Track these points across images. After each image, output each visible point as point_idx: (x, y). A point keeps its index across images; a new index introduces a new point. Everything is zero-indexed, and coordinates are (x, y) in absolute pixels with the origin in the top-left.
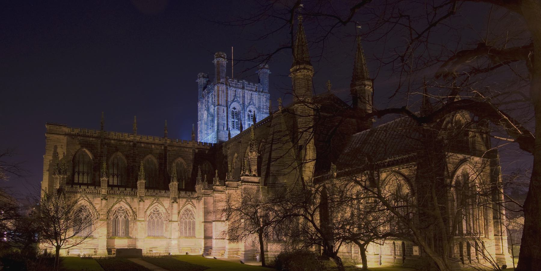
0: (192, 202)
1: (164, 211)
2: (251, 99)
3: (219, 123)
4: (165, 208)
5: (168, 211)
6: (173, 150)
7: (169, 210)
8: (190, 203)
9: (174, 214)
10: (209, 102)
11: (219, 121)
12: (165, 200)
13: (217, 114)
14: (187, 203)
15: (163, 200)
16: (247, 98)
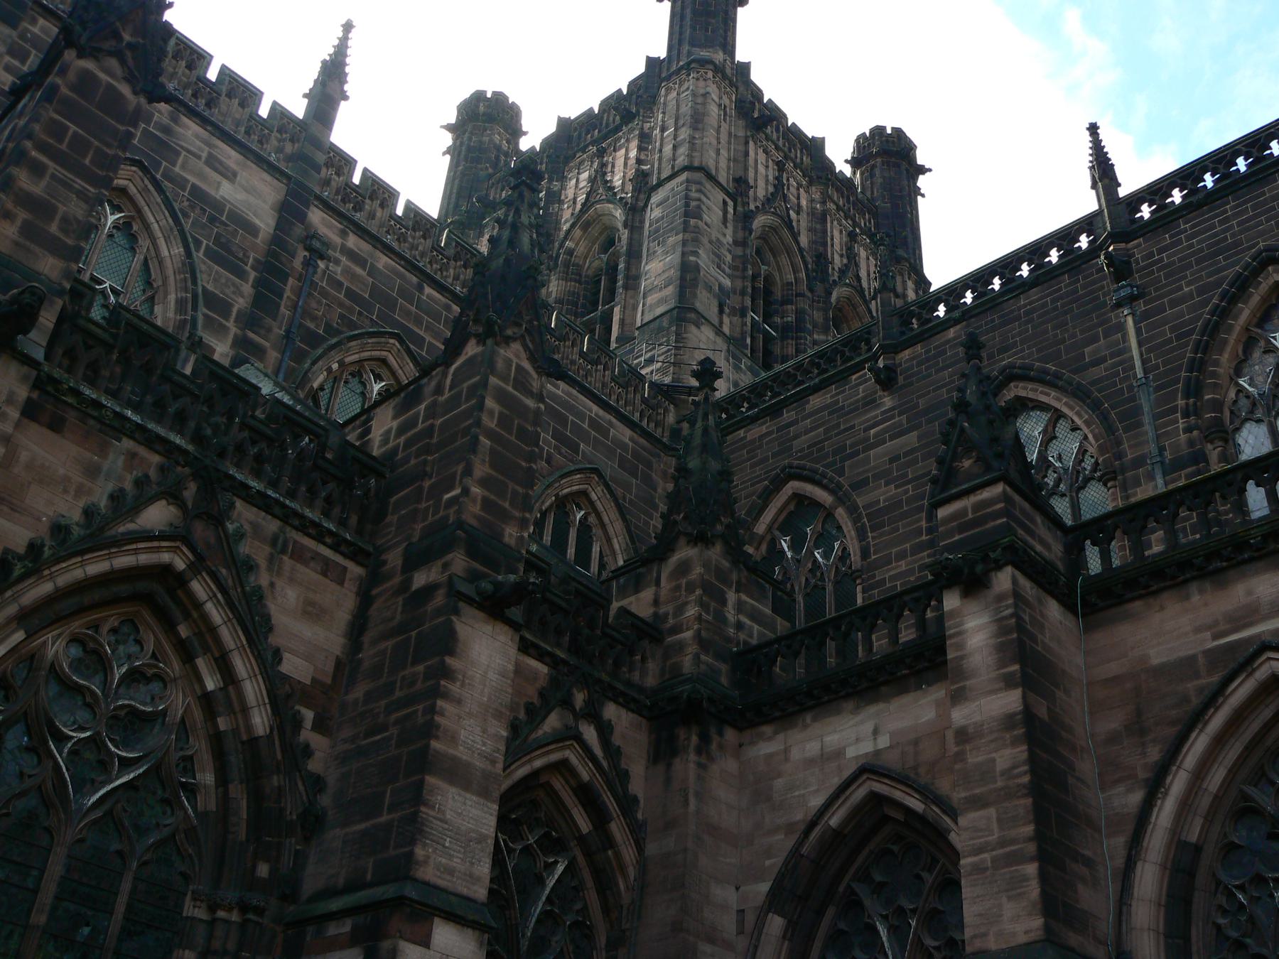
0: (605, 731)
1: (260, 721)
2: (851, 257)
3: (697, 268)
4: (285, 668)
5: (307, 735)
6: (352, 255)
7: (321, 726)
8: (590, 733)
9: (458, 774)
10: (561, 202)
11: (695, 253)
12: (299, 555)
13: (686, 214)
14: (553, 722)
15: (279, 546)
16: (832, 239)
